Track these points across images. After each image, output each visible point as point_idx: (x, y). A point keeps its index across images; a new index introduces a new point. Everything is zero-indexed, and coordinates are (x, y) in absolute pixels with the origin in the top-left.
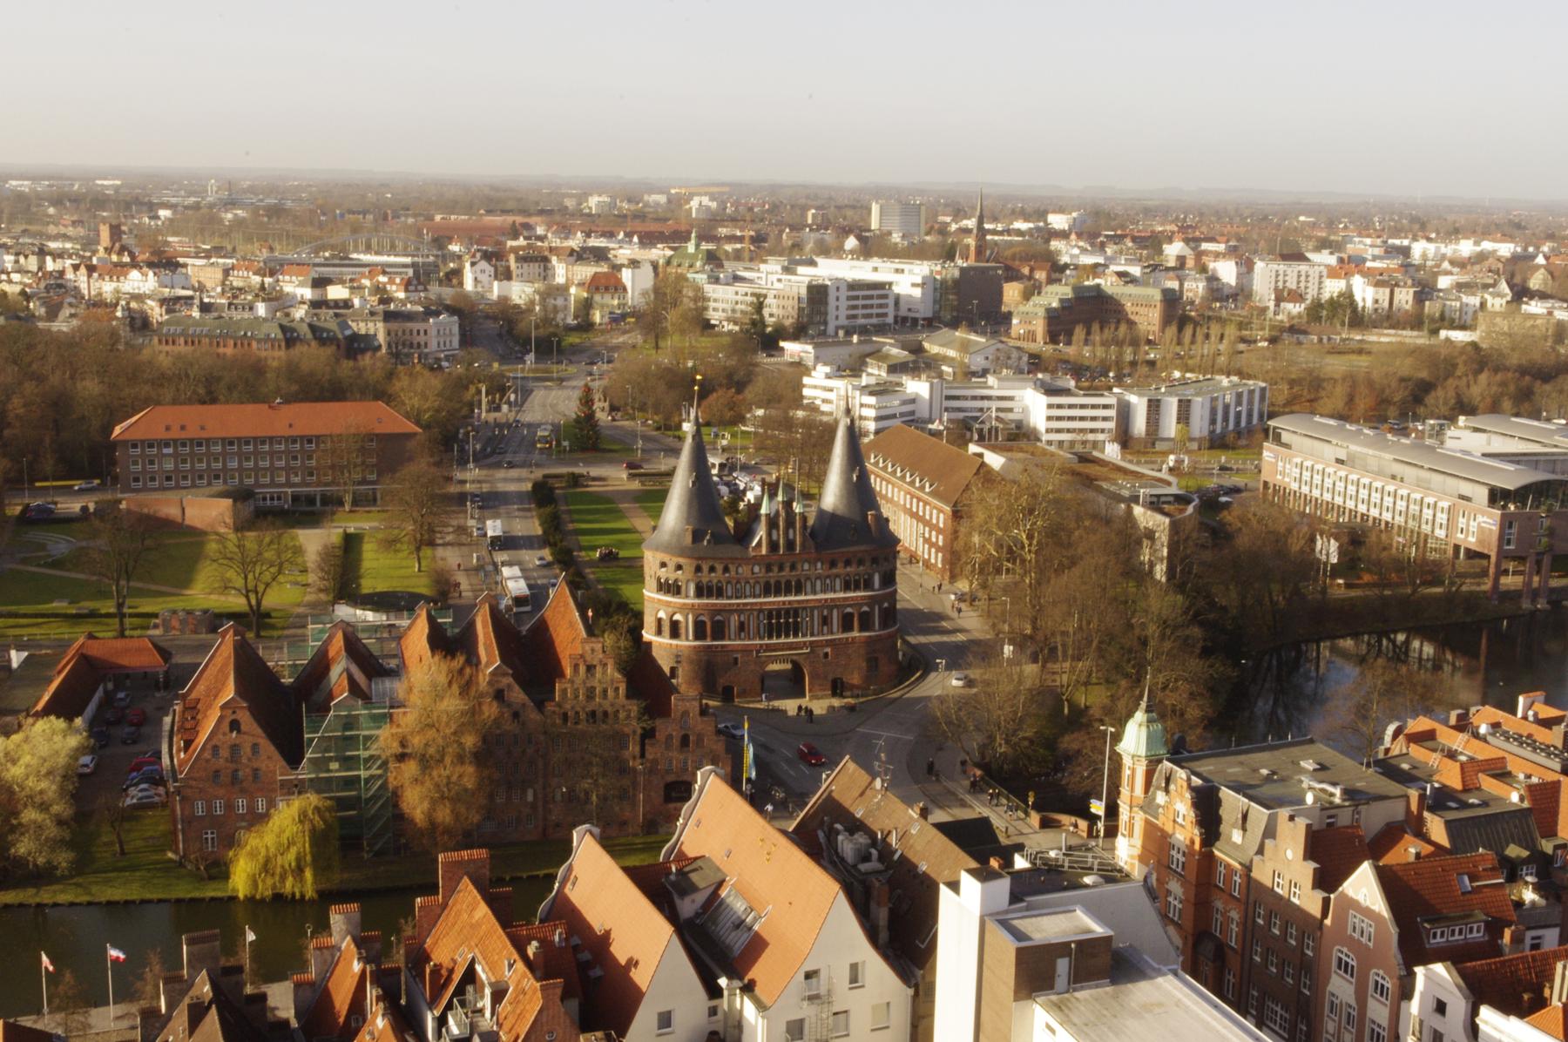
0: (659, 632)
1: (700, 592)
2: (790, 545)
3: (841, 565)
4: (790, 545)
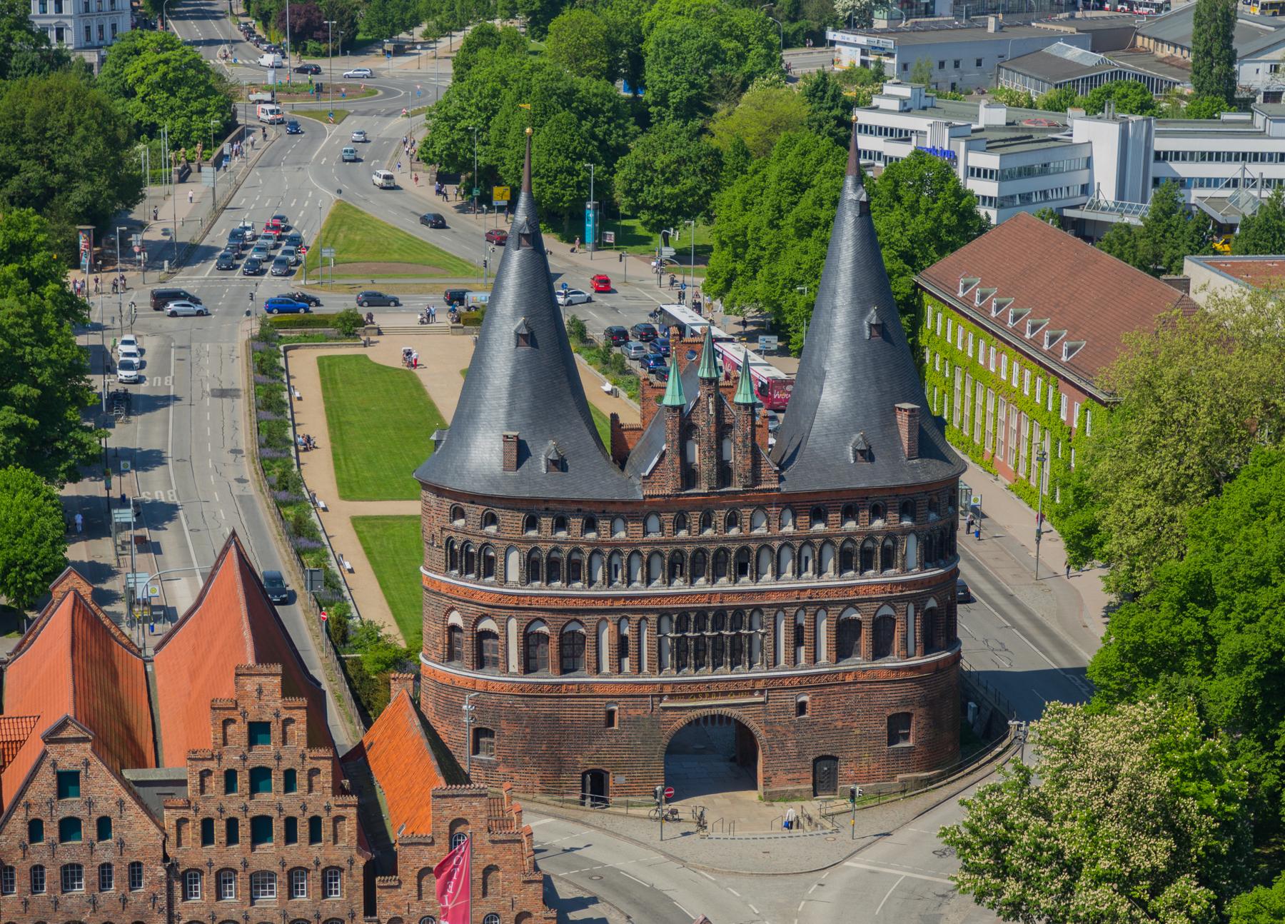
0: (451, 655)
1: (532, 570)
2: (724, 473)
3: (834, 517)
4: (724, 473)
